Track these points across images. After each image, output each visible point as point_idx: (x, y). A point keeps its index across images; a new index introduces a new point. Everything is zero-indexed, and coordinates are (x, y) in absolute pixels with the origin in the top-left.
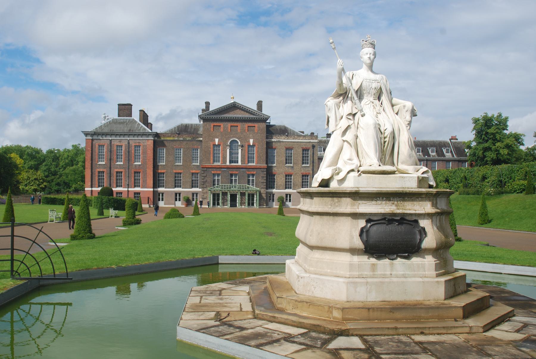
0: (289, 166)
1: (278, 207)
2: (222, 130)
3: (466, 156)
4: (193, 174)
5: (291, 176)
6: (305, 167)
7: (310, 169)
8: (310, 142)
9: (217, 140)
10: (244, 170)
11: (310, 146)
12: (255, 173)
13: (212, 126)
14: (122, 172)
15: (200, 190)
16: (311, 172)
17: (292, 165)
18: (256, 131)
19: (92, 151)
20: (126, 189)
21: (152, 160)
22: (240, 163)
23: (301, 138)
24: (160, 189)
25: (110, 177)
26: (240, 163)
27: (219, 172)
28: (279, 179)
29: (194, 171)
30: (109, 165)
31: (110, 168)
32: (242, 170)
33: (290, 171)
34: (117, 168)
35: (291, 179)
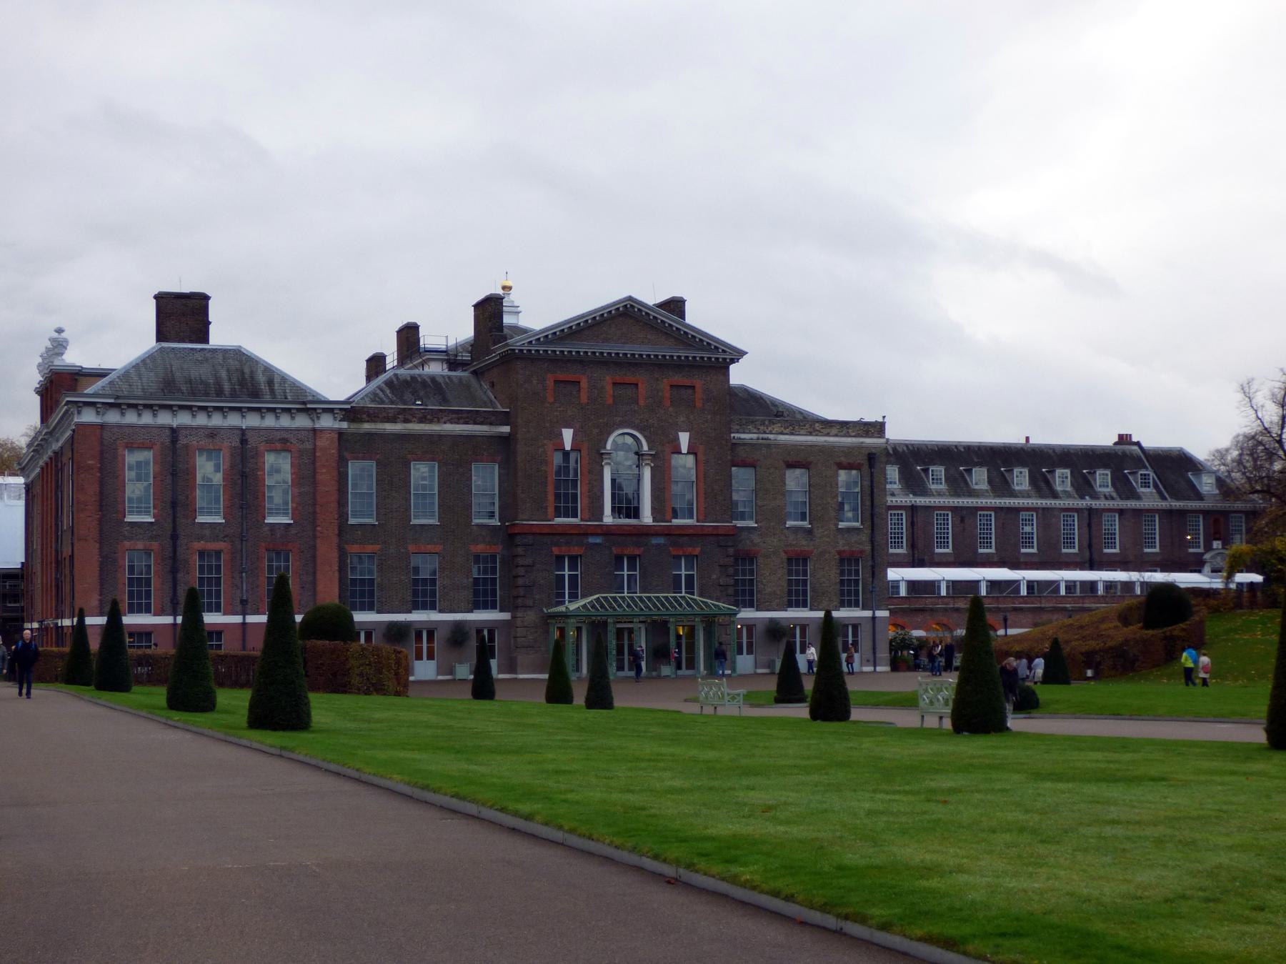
0: (796, 530)
1: (546, 676)
2: (584, 397)
3: (1199, 496)
4: (477, 558)
5: (805, 561)
6: (849, 530)
7: (865, 537)
8: (860, 447)
9: (568, 435)
10: (661, 540)
11: (861, 459)
12: (697, 551)
13: (550, 383)
14: (218, 553)
15: (506, 616)
16: (868, 548)
17: (806, 524)
18: (699, 404)
19: (101, 470)
20: (237, 619)
21: (334, 505)
22: (647, 517)
23: (834, 431)
24: (210, 618)
25: (174, 571)
26: (647, 517)
27: (576, 551)
28: (772, 576)
29: (480, 548)
30: (169, 527)
31: (174, 537)
32: (654, 541)
33: (803, 544)
34: (201, 538)
35: (805, 573)
